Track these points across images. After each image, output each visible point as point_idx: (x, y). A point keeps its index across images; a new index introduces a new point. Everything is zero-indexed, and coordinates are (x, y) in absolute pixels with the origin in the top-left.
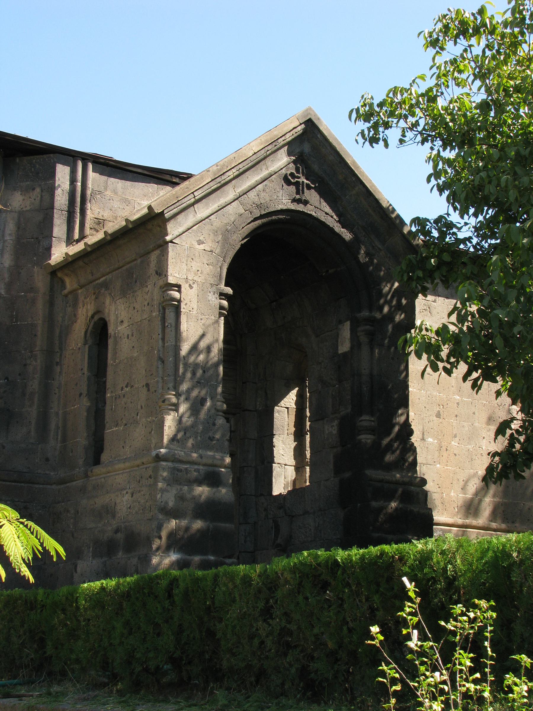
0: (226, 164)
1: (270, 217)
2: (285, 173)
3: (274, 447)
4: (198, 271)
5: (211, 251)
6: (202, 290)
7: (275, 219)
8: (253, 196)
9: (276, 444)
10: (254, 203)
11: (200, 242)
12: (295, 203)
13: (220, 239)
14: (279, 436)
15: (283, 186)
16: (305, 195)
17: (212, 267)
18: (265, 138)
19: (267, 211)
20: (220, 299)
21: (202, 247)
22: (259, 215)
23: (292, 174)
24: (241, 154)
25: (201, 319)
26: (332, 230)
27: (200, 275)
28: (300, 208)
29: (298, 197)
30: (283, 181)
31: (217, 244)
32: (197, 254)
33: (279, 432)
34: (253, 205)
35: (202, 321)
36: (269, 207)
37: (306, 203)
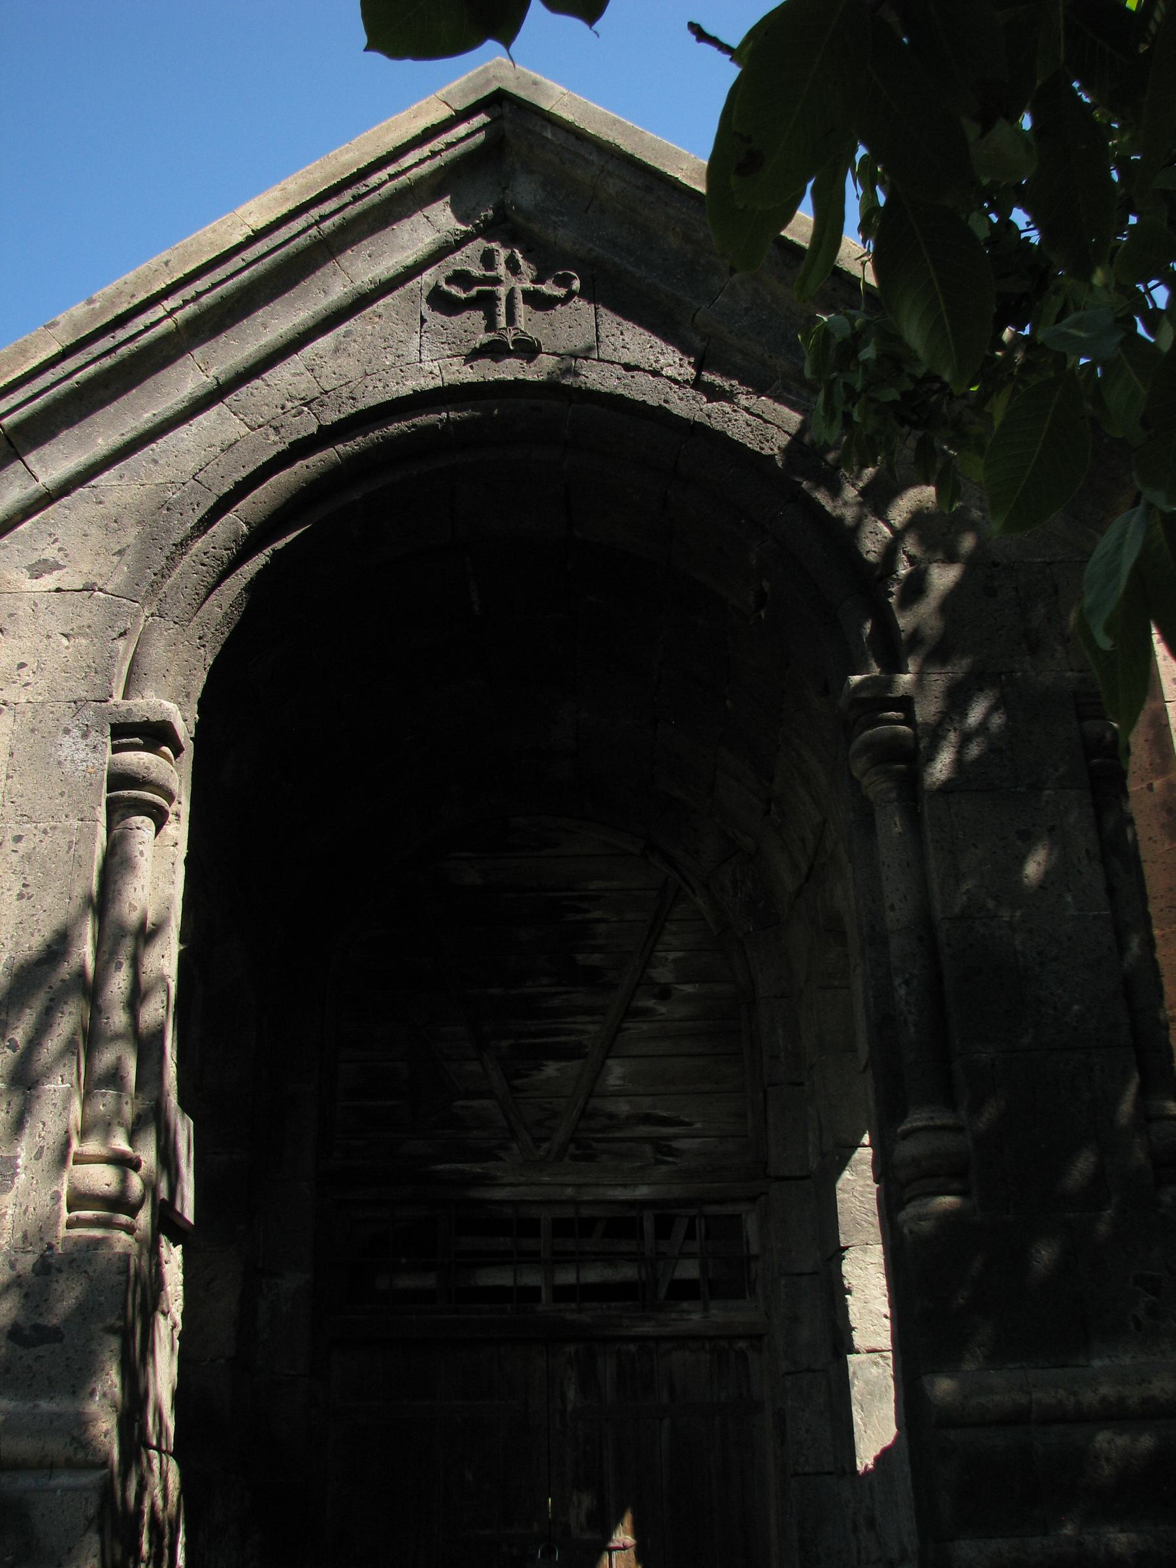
0: (129, 289)
1: (379, 428)
2: (433, 283)
3: (849, 1292)
4: (22, 665)
5: (89, 588)
6: (33, 731)
7: (402, 435)
8: (287, 376)
9: (854, 1282)
10: (291, 398)
11: (38, 570)
12: (486, 362)
13: (131, 540)
14: (865, 1251)
15: (423, 321)
16: (521, 323)
17: (84, 642)
18: (301, 181)
19: (349, 410)
20: (116, 749)
21: (49, 581)
22: (314, 429)
23: (461, 278)
24: (194, 248)
25: (18, 839)
26: (660, 416)
27: (31, 679)
28: (510, 370)
29: (483, 338)
30: (425, 307)
31: (116, 559)
32: (24, 609)
33: (863, 1237)
34: (289, 405)
35: (22, 846)
36: (358, 396)
37: (528, 350)
